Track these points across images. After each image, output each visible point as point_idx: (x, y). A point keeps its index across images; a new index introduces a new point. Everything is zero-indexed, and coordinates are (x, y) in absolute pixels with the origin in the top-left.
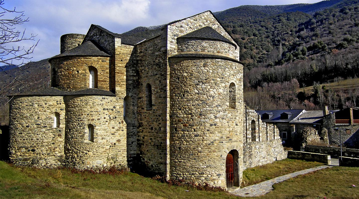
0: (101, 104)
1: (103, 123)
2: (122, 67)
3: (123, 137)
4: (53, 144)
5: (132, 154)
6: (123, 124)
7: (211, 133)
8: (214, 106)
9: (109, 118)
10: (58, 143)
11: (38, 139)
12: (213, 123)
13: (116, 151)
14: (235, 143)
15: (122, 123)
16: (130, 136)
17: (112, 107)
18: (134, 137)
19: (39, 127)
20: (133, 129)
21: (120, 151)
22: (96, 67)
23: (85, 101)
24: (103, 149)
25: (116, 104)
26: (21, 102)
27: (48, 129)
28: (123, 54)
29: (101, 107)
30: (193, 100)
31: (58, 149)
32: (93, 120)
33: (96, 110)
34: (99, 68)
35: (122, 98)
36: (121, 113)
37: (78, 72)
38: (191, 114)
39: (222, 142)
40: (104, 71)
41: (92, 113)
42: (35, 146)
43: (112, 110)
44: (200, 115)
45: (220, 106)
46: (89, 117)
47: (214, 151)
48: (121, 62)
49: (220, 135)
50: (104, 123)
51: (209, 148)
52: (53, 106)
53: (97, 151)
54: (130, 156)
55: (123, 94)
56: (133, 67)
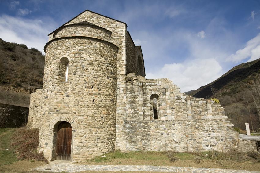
14: (66, 114)
39: (50, 113)
49: (49, 106)
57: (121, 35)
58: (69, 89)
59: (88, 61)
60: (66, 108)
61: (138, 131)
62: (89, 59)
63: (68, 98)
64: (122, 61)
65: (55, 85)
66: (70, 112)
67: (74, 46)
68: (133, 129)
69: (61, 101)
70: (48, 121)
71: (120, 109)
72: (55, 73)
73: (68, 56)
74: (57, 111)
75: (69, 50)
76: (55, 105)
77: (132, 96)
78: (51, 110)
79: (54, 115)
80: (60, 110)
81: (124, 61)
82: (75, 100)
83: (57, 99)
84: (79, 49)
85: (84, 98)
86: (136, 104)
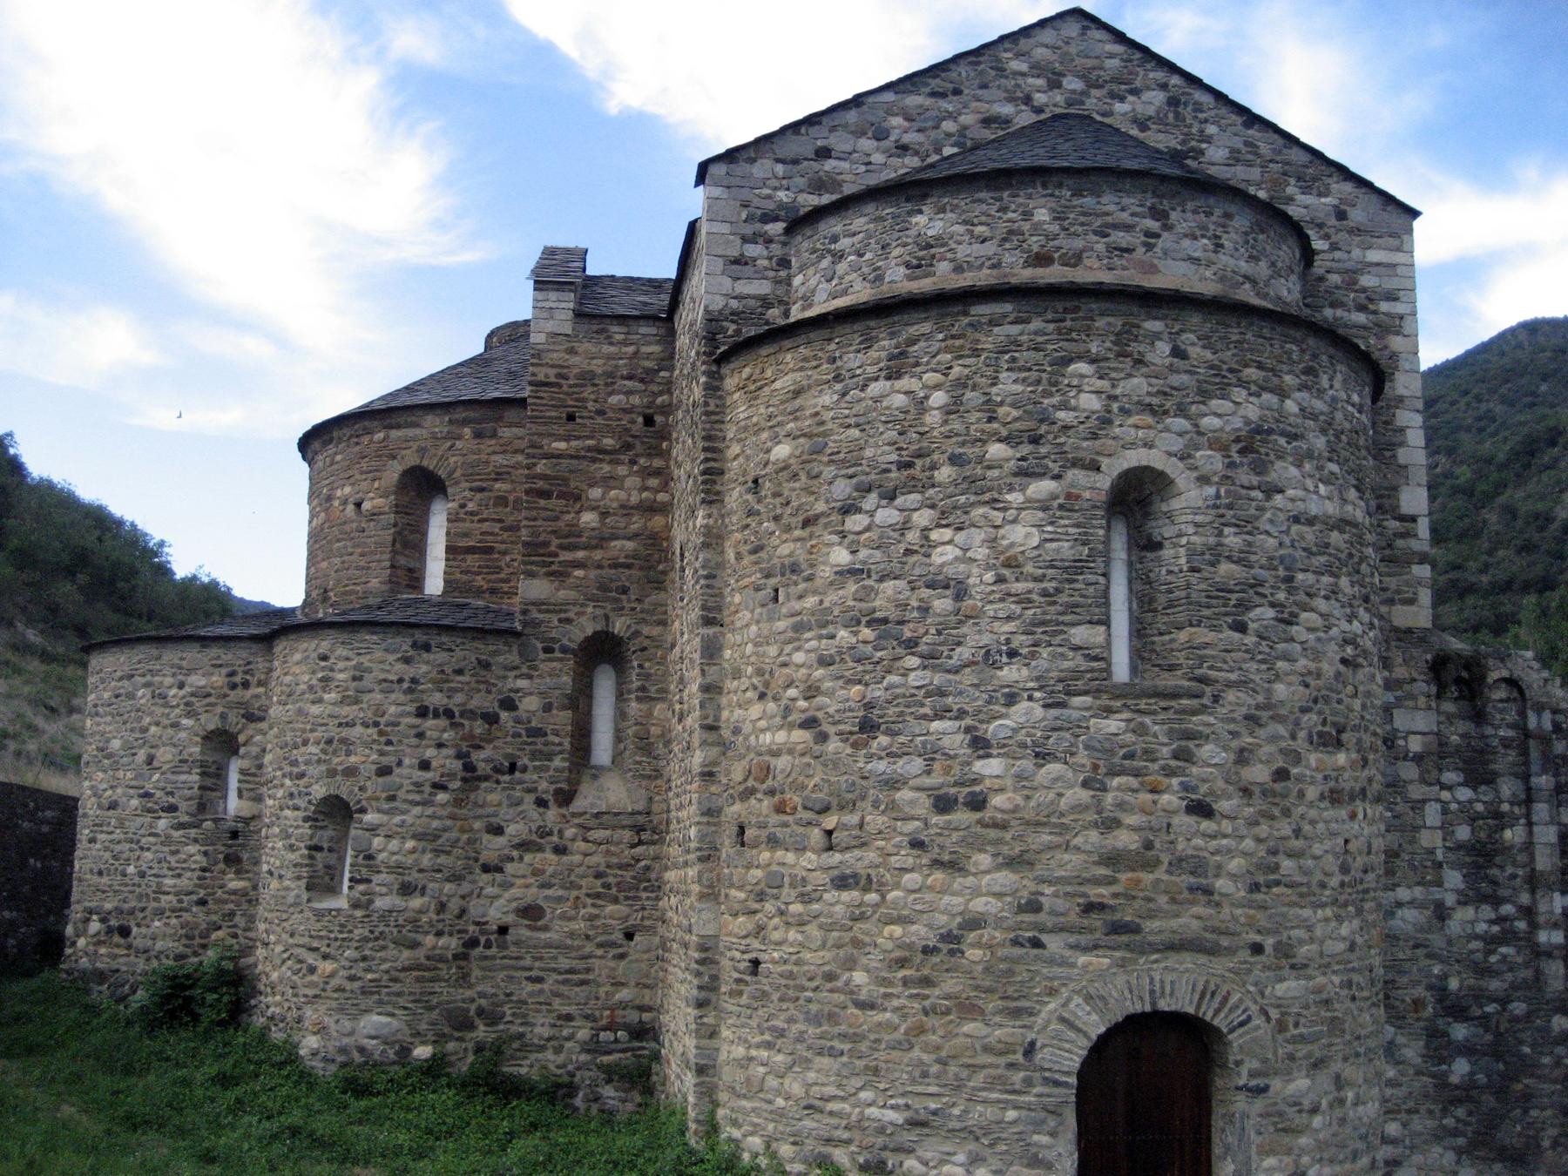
0: (400, 681)
1: (411, 797)
2: (572, 457)
3: (560, 892)
4: (202, 902)
5: (623, 1005)
6: (563, 811)
7: (937, 863)
8: (964, 653)
9: (457, 765)
10: (226, 902)
11: (142, 875)
12: (953, 791)
13: (512, 973)
14: (1187, 960)
15: (556, 801)
16: (614, 891)
17: (479, 702)
18: (644, 895)
19: (149, 811)
20: (633, 846)
21: (539, 980)
22: (442, 473)
23: (323, 664)
24: (406, 953)
25: (522, 683)
27: (186, 818)
28: (587, 377)
29: (402, 698)
30: (824, 625)
31: (220, 934)
32: (351, 772)
33: (370, 714)
34: (457, 474)
35: (564, 650)
36: (551, 738)
38: (809, 723)
39: (1037, 944)
40: (481, 490)
41: (345, 732)
42: (132, 912)
43: (491, 719)
44: (868, 727)
45: (1012, 654)
46: (335, 752)
47: (969, 1010)
48: (570, 426)
49: (1005, 878)
50: (417, 798)
51: (927, 982)
52: (208, 700)
53: (364, 959)
54: (612, 1016)
55: (568, 621)
56: (650, 455)
57: (1384, 306)
58: (1207, 751)
59: (1311, 522)
60: (1193, 903)
61: (1532, 1076)
62: (1314, 508)
63: (1206, 825)
64: (1403, 518)
65: (1077, 701)
66: (1225, 941)
67: (1218, 384)
68: (1498, 1056)
69: (1148, 846)
70: (1016, 1013)
71: (1399, 904)
72: (1063, 598)
73: (1181, 465)
74: (1117, 928)
75: (1182, 411)
76: (1097, 882)
77: (1480, 807)
78: (1042, 917)
79: (1083, 959)
80: (1150, 925)
81: (1413, 519)
82: (1248, 844)
83: (1109, 824)
84: (1252, 411)
85: (1307, 828)
86: (1509, 870)
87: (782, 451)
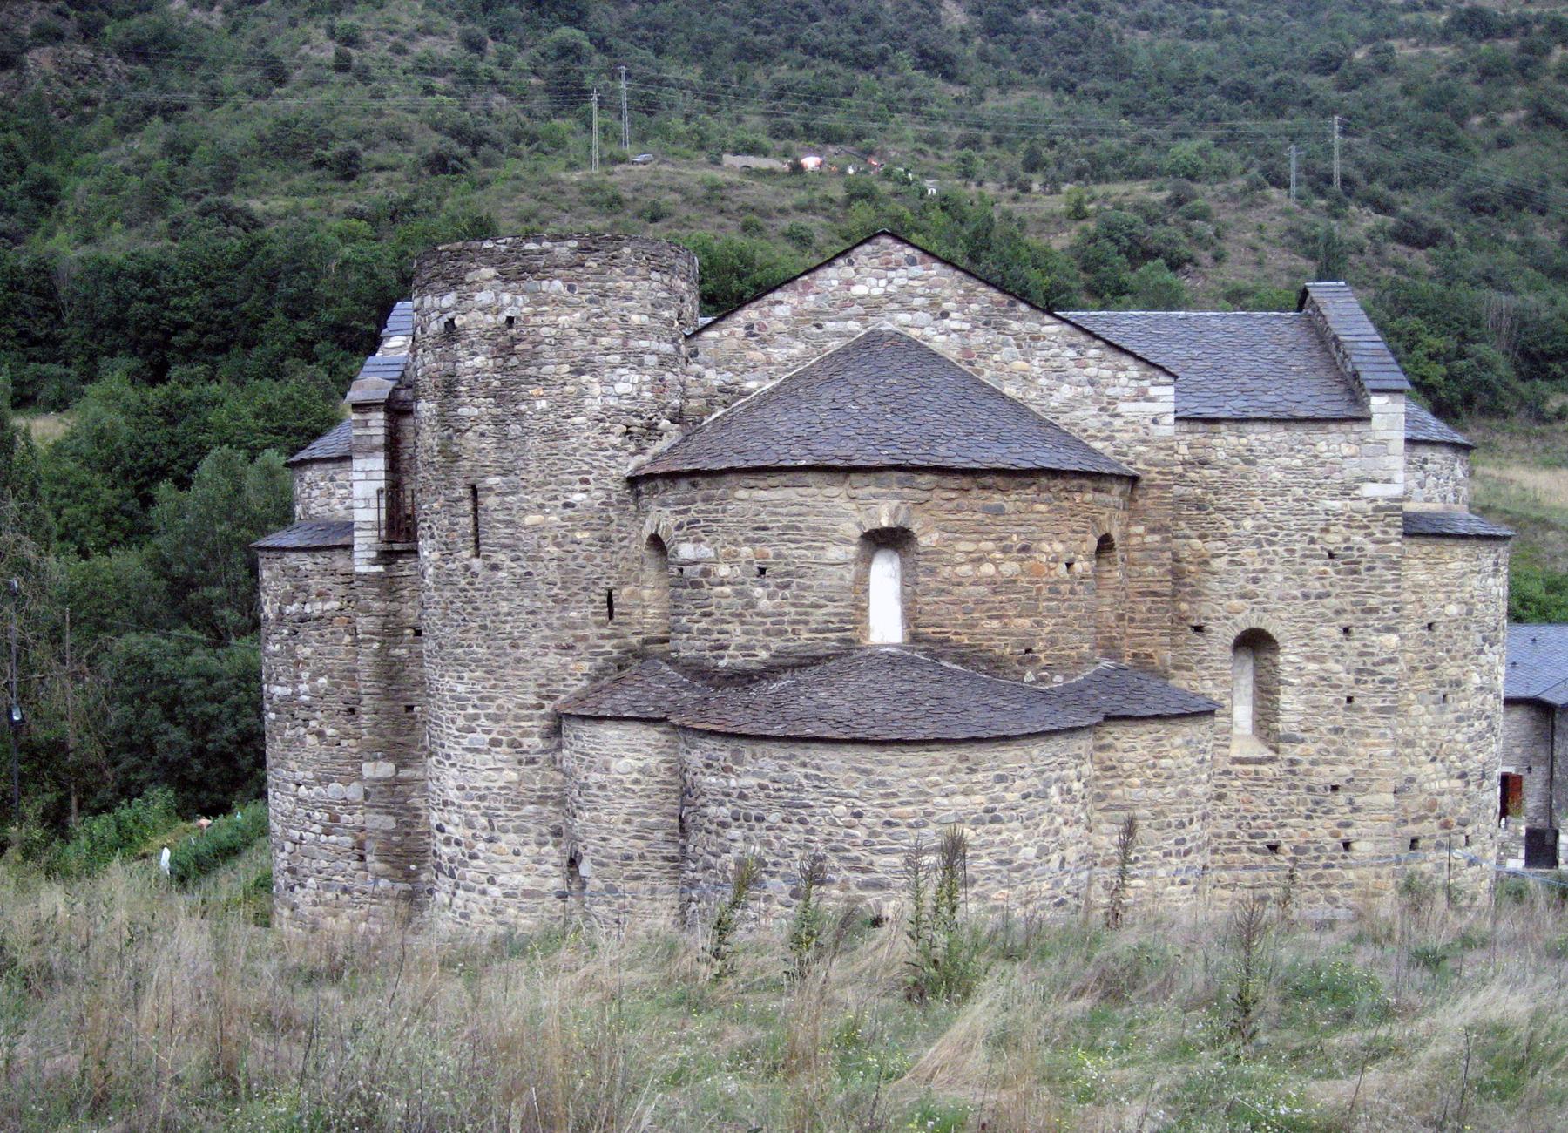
26: (1001, 779)
37: (1069, 565)
38: (1463, 776)
87: (1453, 609)
